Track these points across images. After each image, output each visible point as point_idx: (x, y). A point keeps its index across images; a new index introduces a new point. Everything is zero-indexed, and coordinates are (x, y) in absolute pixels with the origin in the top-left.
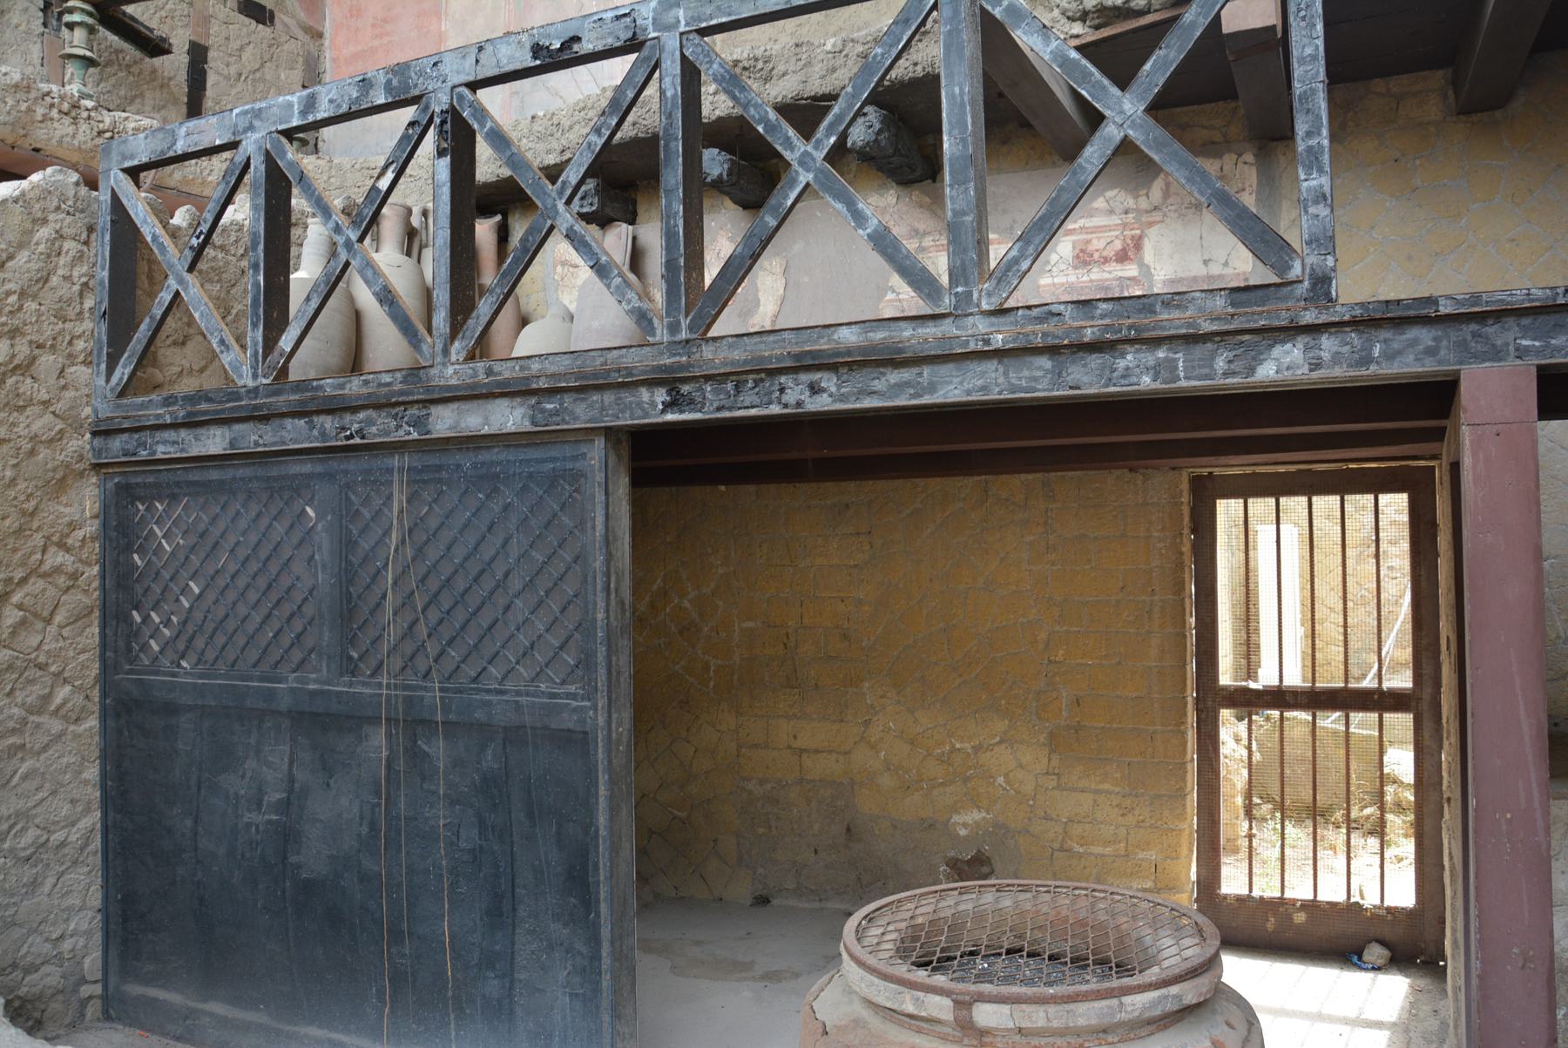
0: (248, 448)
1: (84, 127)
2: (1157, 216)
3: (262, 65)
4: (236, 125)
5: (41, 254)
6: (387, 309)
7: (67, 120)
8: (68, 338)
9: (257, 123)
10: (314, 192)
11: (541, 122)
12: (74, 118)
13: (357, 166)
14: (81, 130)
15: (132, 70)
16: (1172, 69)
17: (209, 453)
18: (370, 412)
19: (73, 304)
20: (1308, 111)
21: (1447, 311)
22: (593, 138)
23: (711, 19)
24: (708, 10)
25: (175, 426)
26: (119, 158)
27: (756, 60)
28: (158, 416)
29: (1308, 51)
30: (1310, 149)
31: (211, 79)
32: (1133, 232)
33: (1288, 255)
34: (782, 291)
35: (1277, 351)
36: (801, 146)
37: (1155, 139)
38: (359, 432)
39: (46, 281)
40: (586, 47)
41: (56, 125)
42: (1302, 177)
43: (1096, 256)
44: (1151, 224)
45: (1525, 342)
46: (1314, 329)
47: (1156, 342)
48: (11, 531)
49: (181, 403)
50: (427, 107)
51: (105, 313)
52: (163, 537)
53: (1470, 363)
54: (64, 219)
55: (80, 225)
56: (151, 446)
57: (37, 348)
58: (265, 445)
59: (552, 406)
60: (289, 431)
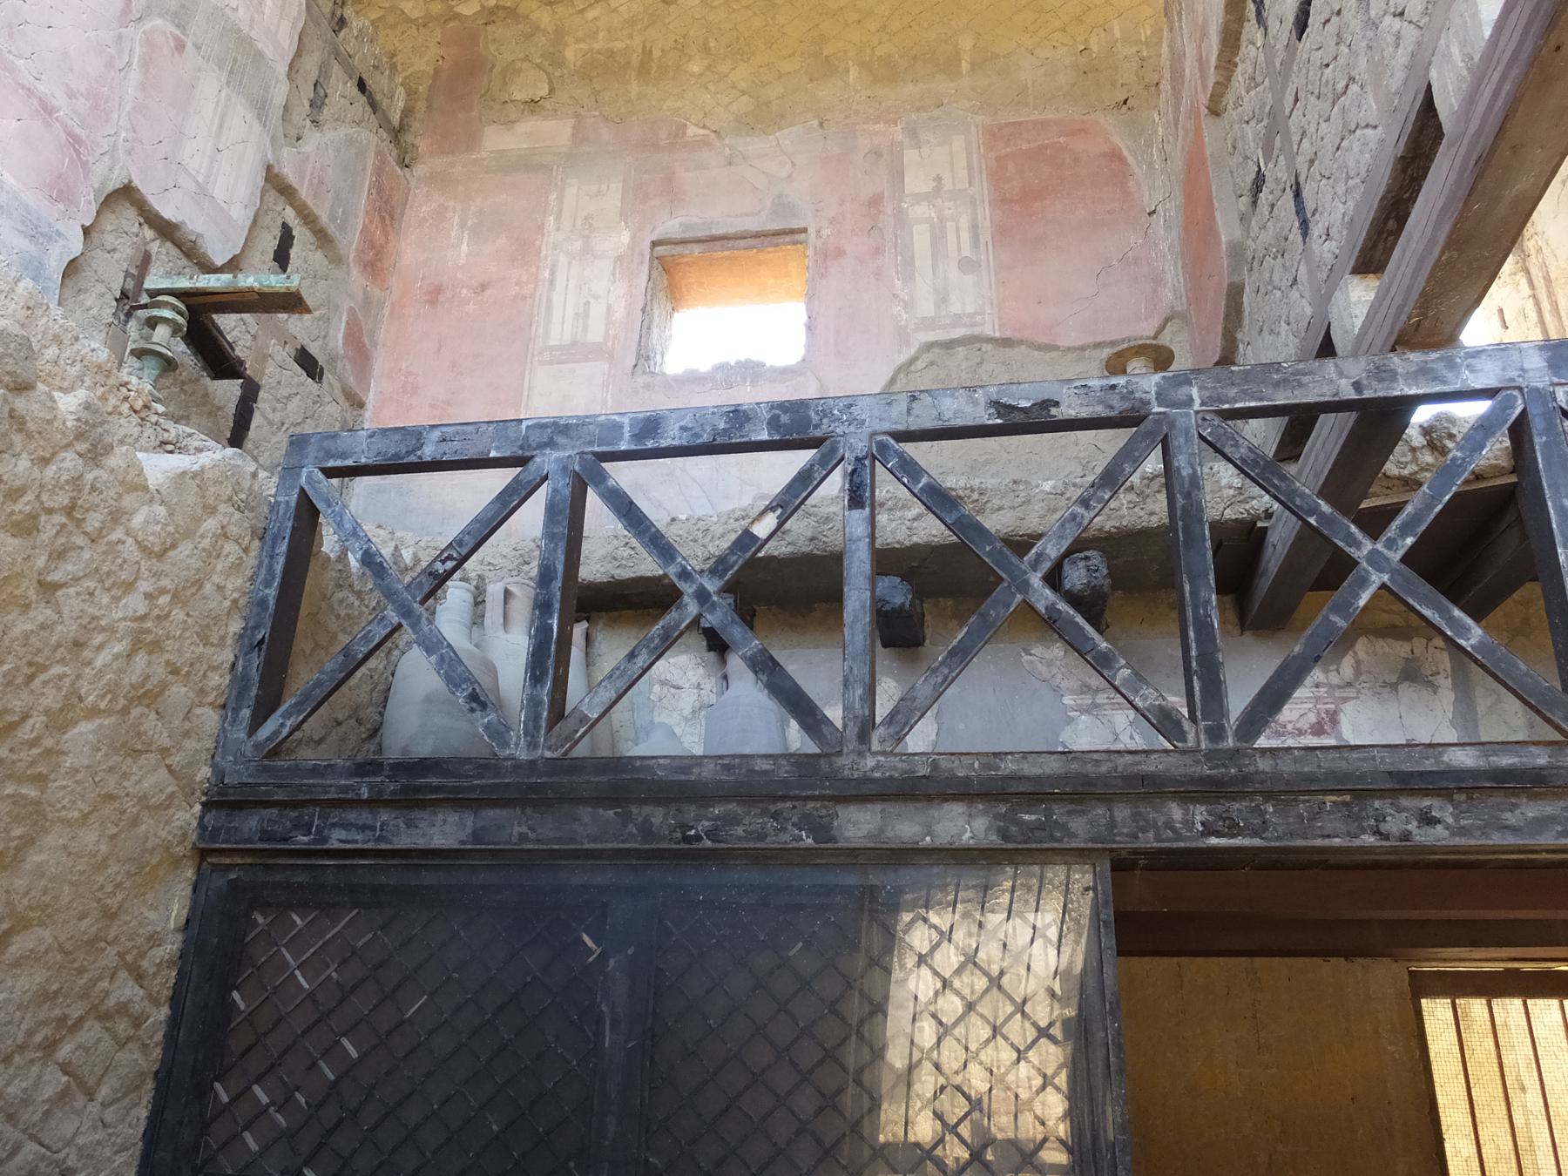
0: (509, 843)
1: (149, 431)
2: (1350, 692)
3: (304, 421)
4: (526, 438)
5: (204, 550)
6: (765, 678)
7: (135, 419)
8: (205, 667)
9: (561, 440)
10: (648, 528)
11: (681, 525)
12: (143, 419)
13: (422, 544)
14: (145, 435)
15: (185, 387)
17: (432, 846)
18: (732, 806)
19: (220, 623)
22: (1080, 510)
23: (1236, 402)
24: (1232, 392)
25: (374, 803)
26: (321, 454)
27: (973, 490)
28: (346, 789)
31: (257, 420)
32: (1327, 706)
34: (933, 737)
36: (1368, 545)
38: (711, 833)
39: (200, 588)
40: (1066, 411)
41: (122, 421)
43: (1290, 727)
44: (1345, 700)
48: (85, 938)
49: (386, 773)
50: (834, 450)
51: (261, 642)
52: (298, 968)
54: (232, 514)
55: (246, 525)
56: (320, 830)
57: (171, 673)
58: (538, 841)
59: (1033, 817)
60: (586, 825)
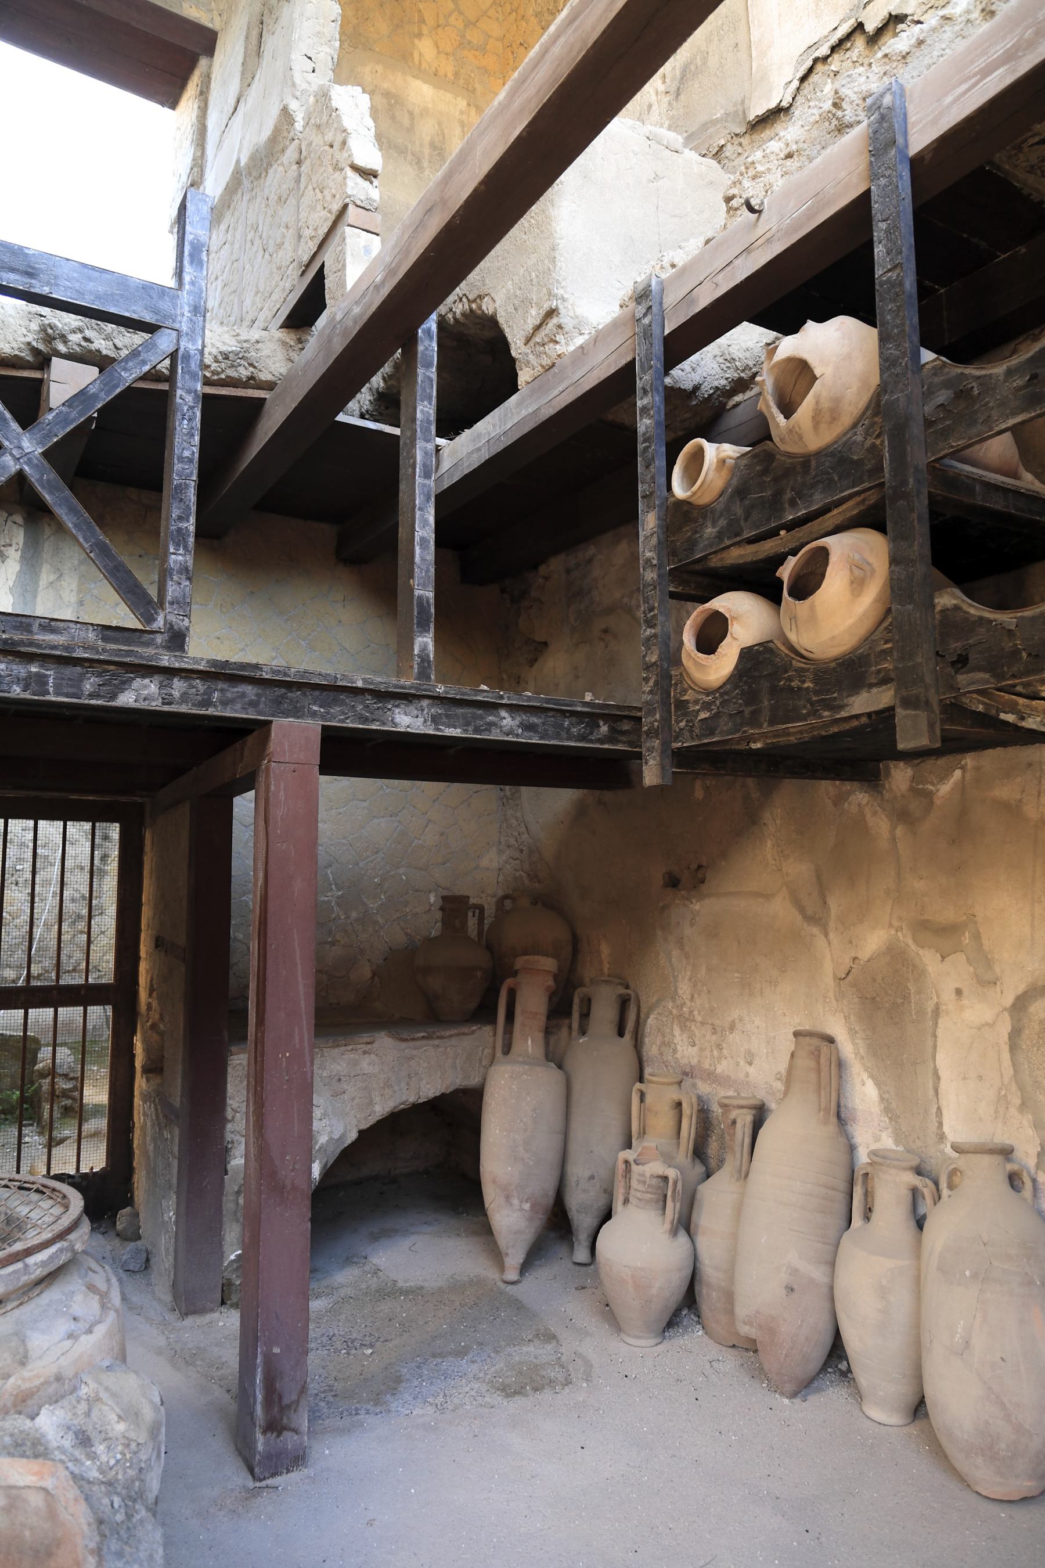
16: (72, 427)
20: (181, 500)
21: (267, 677)
29: (186, 454)
30: (179, 530)
33: (154, 609)
35: (138, 683)
37: (48, 481)
42: (172, 550)
45: (315, 708)
46: (170, 672)
47: (30, 658)
53: (279, 717)
